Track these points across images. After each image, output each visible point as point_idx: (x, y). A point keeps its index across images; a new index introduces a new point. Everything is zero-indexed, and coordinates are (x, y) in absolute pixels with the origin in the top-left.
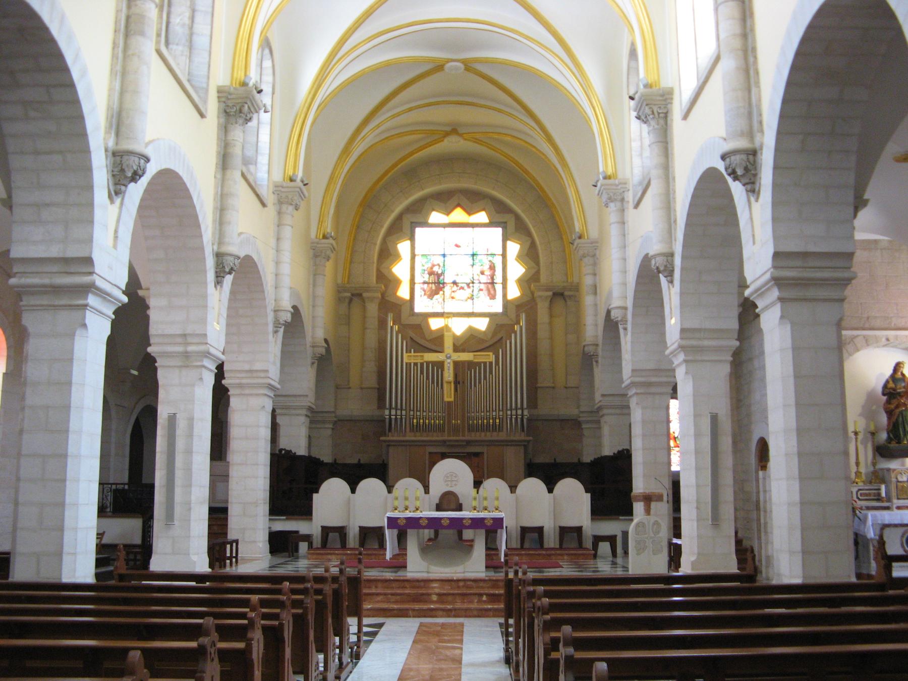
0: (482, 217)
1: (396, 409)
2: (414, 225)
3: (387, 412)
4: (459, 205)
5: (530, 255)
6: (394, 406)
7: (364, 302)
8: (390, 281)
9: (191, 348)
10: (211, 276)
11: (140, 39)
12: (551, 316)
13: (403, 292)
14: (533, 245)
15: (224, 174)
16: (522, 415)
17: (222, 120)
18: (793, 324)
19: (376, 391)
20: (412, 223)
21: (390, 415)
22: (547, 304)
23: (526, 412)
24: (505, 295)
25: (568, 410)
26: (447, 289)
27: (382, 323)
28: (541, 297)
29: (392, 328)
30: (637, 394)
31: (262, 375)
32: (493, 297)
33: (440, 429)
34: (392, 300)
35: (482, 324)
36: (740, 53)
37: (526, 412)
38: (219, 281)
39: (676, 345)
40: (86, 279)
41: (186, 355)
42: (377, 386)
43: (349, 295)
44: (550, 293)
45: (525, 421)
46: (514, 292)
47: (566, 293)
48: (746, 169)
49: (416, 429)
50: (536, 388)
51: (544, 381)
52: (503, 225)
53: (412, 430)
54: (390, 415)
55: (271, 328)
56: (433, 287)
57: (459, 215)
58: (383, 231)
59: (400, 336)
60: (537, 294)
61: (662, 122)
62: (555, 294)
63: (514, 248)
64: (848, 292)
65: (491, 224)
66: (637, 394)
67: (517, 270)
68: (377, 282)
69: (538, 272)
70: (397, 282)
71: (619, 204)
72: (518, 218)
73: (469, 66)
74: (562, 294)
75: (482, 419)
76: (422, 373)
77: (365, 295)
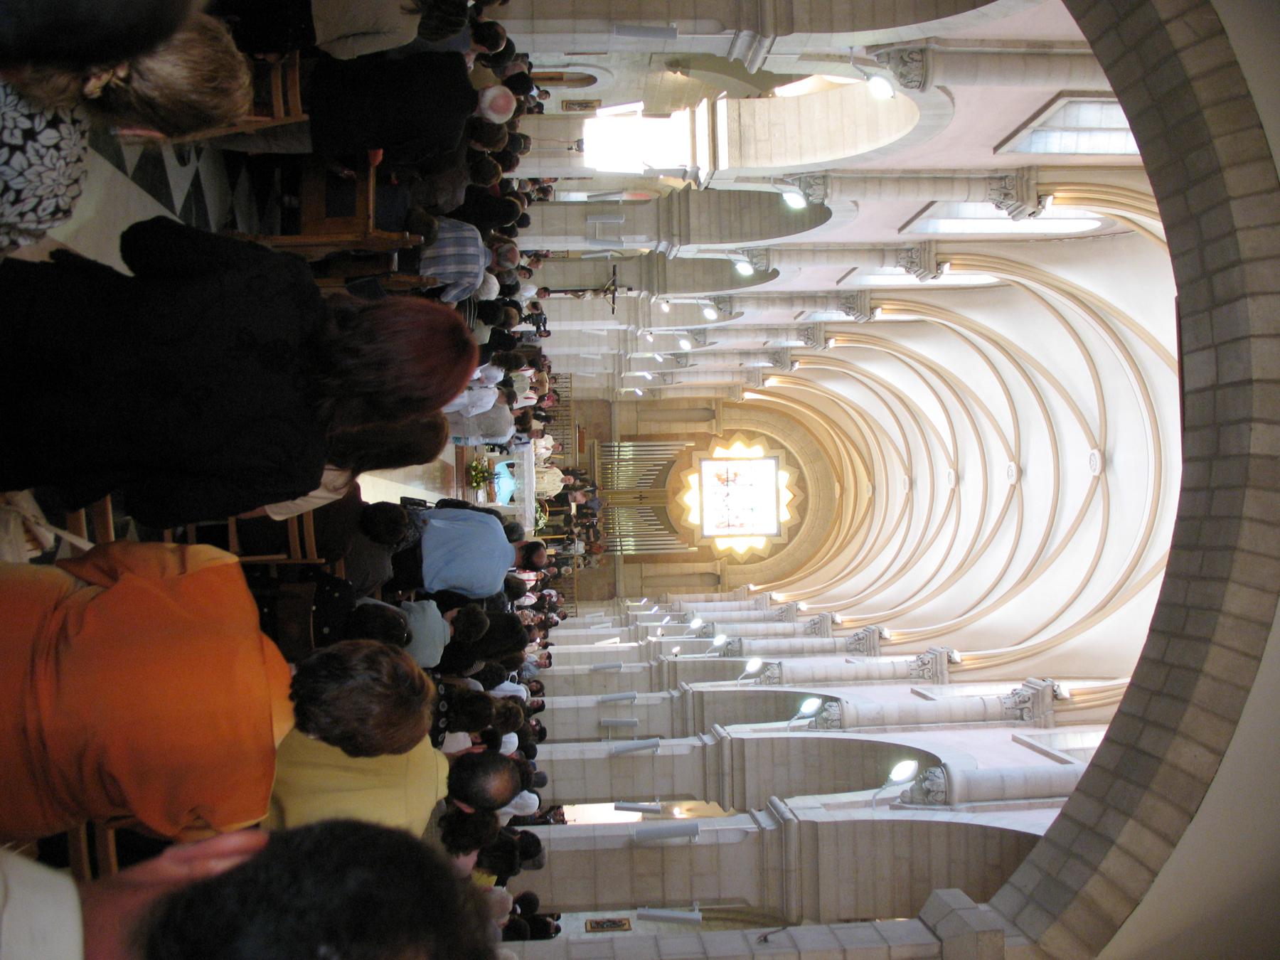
0: (786, 516)
1: (619, 451)
2: (776, 458)
3: (616, 444)
4: (795, 496)
5: (754, 558)
6: (621, 449)
7: (708, 420)
8: (728, 440)
9: (629, 343)
10: (672, 352)
11: (765, 337)
12: (702, 574)
13: (719, 451)
14: (762, 559)
15: (736, 354)
16: (617, 550)
17: (770, 351)
18: (629, 651)
19: (635, 433)
20: (778, 457)
21: (614, 447)
22: (710, 570)
23: (619, 553)
24: (718, 536)
25: (621, 588)
26: (724, 489)
27: (692, 436)
28: (715, 566)
29: (682, 445)
30: (621, 618)
31: (628, 368)
32: (718, 527)
33: (604, 487)
34: (713, 442)
35: (693, 519)
36: (765, 632)
37: (619, 553)
38: (671, 354)
39: (724, 734)
40: (641, 325)
41: (625, 341)
42: (639, 434)
43: (714, 408)
44: (719, 573)
45: (612, 553)
46: (721, 545)
47: (719, 586)
48: (705, 633)
49: (604, 468)
50: (640, 563)
51: (649, 569)
52: (779, 535)
53: (603, 464)
54: (614, 447)
55: (660, 371)
56: (724, 477)
57: (787, 496)
58: (769, 434)
59: (677, 452)
60: (718, 563)
61: (777, 618)
62: (719, 577)
63: (760, 545)
64: (714, 805)
65: (779, 525)
66: (621, 618)
67: (741, 547)
68: (724, 430)
69: (739, 564)
70: (727, 447)
71: (754, 606)
72: (785, 545)
73: (872, 502)
74: (719, 583)
75: (613, 519)
76: (648, 471)
77: (714, 421)
